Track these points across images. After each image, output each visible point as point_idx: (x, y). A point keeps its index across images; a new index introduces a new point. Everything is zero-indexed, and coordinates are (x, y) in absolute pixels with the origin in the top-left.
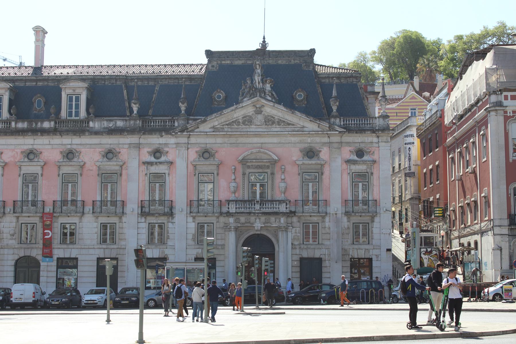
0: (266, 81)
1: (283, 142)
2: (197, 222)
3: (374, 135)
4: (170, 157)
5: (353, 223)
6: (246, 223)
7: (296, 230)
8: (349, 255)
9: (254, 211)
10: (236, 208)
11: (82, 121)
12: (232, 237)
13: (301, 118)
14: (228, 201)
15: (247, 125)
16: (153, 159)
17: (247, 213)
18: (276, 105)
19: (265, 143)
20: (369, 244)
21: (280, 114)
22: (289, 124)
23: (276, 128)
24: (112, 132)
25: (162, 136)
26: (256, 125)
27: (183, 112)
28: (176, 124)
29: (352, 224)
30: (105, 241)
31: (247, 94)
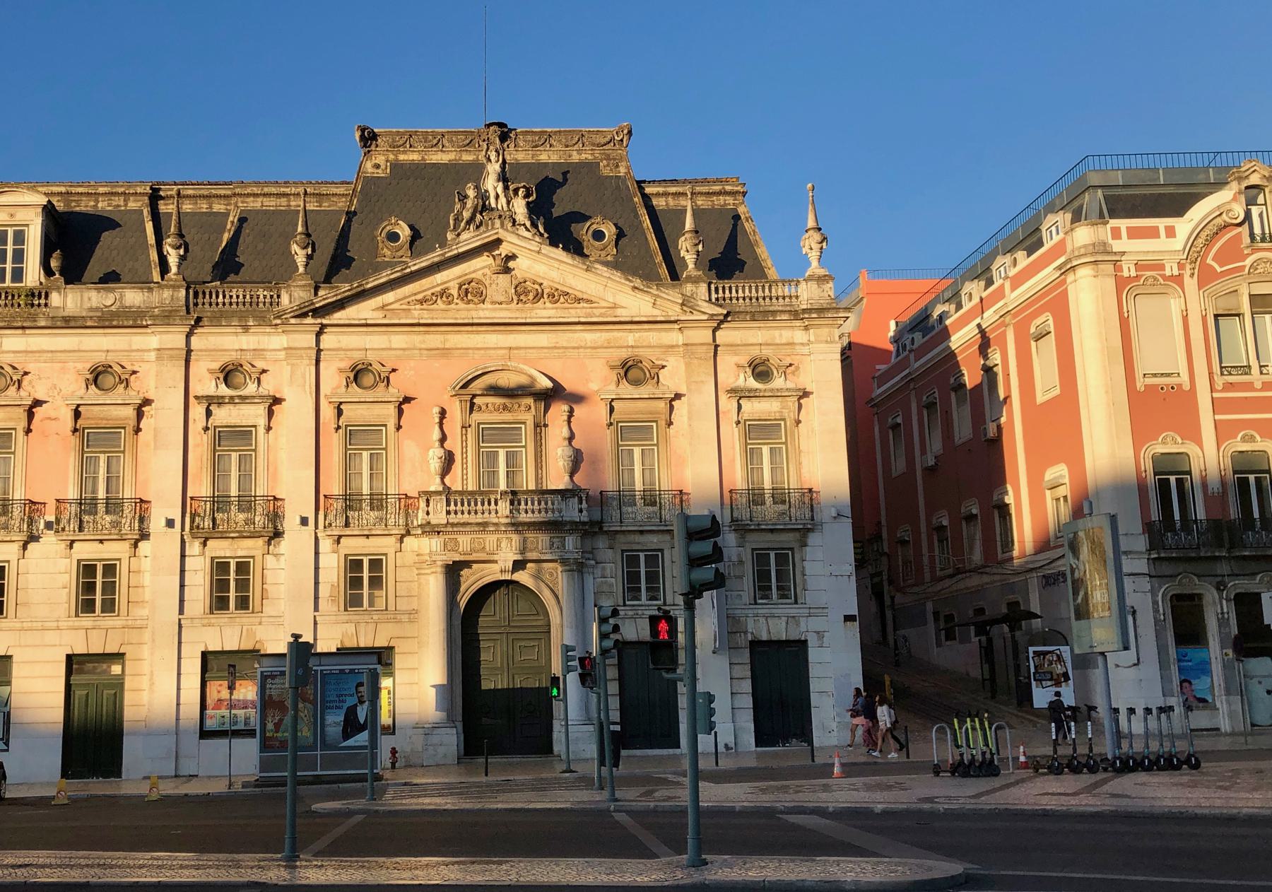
0: (516, 191)
1: (565, 344)
2: (343, 551)
3: (798, 323)
4: (269, 386)
5: (753, 550)
6: (473, 550)
7: (604, 569)
8: (746, 633)
9: (495, 520)
10: (448, 513)
11: (31, 294)
12: (434, 586)
13: (610, 284)
14: (426, 493)
15: (469, 302)
16: (224, 390)
17: (478, 524)
18: (547, 249)
19: (517, 348)
20: (796, 602)
21: (554, 275)
22: (579, 300)
23: (544, 311)
24: (107, 321)
25: (246, 328)
26: (493, 303)
27: (301, 269)
28: (285, 299)
29: (749, 551)
30: (87, 606)
31: (468, 223)
